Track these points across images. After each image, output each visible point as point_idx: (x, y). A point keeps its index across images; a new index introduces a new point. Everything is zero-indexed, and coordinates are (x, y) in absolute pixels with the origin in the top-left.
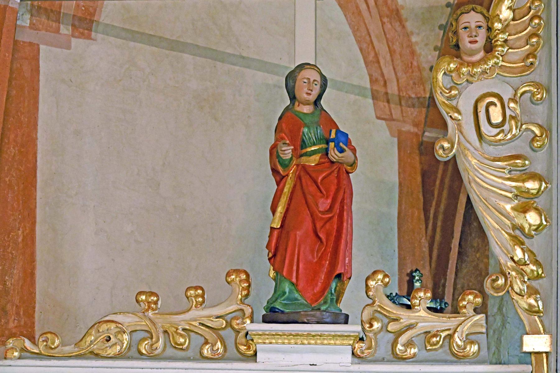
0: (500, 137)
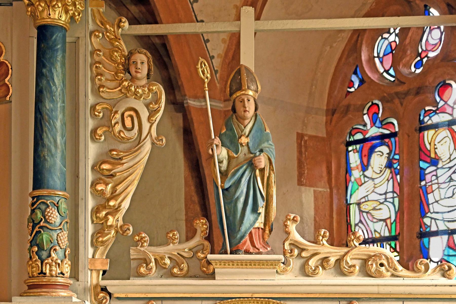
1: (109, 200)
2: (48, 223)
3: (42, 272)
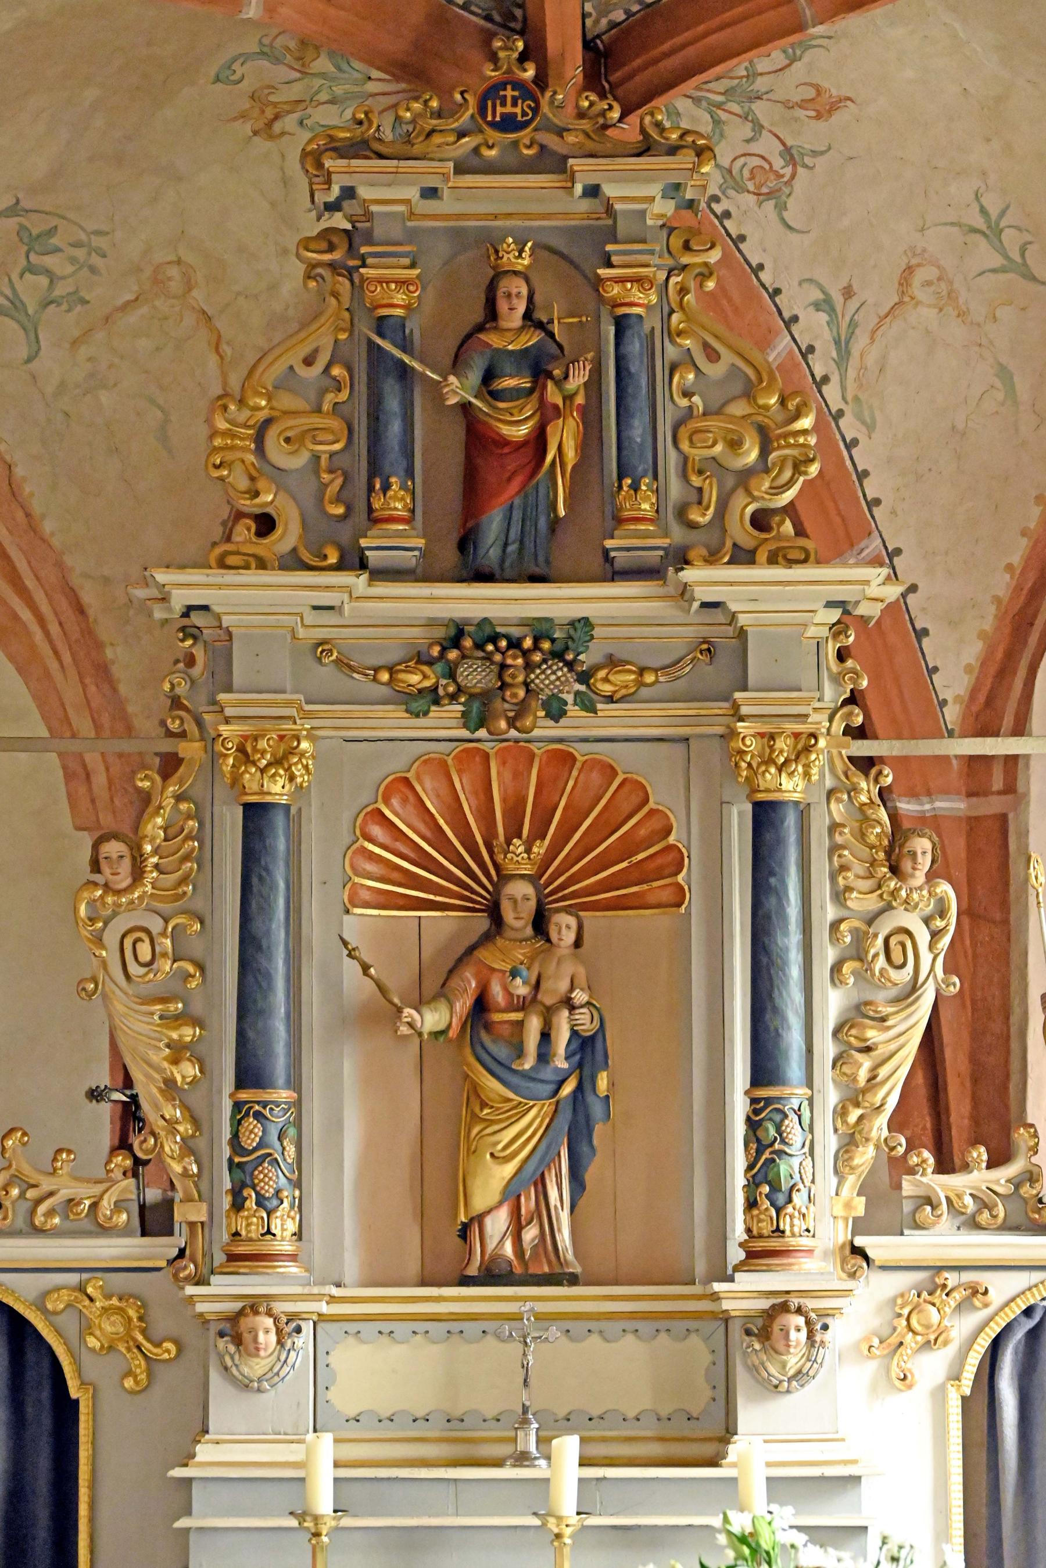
0: (151, 976)
1: (864, 1091)
2: (786, 1144)
3: (778, 1229)
